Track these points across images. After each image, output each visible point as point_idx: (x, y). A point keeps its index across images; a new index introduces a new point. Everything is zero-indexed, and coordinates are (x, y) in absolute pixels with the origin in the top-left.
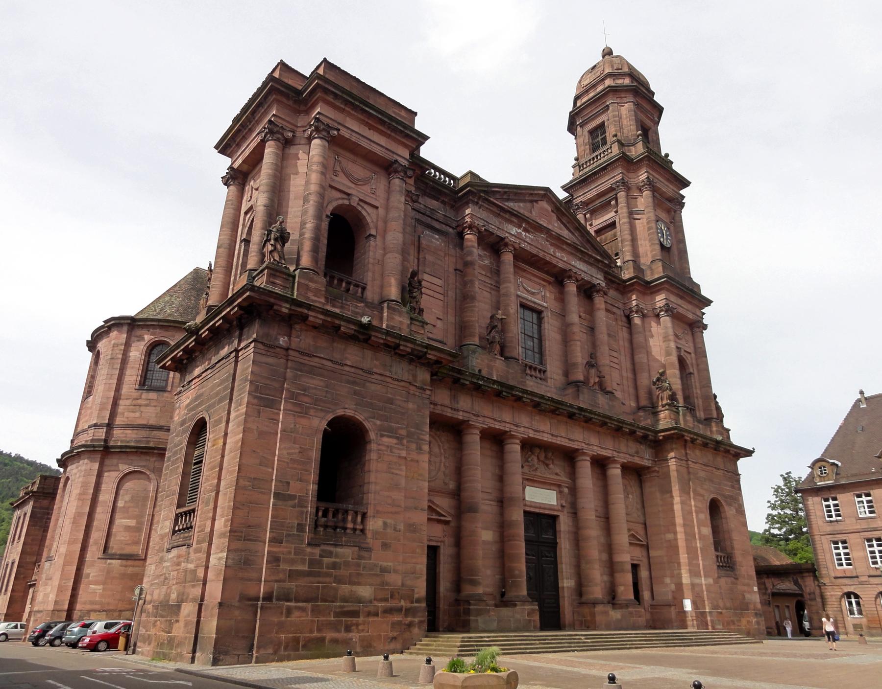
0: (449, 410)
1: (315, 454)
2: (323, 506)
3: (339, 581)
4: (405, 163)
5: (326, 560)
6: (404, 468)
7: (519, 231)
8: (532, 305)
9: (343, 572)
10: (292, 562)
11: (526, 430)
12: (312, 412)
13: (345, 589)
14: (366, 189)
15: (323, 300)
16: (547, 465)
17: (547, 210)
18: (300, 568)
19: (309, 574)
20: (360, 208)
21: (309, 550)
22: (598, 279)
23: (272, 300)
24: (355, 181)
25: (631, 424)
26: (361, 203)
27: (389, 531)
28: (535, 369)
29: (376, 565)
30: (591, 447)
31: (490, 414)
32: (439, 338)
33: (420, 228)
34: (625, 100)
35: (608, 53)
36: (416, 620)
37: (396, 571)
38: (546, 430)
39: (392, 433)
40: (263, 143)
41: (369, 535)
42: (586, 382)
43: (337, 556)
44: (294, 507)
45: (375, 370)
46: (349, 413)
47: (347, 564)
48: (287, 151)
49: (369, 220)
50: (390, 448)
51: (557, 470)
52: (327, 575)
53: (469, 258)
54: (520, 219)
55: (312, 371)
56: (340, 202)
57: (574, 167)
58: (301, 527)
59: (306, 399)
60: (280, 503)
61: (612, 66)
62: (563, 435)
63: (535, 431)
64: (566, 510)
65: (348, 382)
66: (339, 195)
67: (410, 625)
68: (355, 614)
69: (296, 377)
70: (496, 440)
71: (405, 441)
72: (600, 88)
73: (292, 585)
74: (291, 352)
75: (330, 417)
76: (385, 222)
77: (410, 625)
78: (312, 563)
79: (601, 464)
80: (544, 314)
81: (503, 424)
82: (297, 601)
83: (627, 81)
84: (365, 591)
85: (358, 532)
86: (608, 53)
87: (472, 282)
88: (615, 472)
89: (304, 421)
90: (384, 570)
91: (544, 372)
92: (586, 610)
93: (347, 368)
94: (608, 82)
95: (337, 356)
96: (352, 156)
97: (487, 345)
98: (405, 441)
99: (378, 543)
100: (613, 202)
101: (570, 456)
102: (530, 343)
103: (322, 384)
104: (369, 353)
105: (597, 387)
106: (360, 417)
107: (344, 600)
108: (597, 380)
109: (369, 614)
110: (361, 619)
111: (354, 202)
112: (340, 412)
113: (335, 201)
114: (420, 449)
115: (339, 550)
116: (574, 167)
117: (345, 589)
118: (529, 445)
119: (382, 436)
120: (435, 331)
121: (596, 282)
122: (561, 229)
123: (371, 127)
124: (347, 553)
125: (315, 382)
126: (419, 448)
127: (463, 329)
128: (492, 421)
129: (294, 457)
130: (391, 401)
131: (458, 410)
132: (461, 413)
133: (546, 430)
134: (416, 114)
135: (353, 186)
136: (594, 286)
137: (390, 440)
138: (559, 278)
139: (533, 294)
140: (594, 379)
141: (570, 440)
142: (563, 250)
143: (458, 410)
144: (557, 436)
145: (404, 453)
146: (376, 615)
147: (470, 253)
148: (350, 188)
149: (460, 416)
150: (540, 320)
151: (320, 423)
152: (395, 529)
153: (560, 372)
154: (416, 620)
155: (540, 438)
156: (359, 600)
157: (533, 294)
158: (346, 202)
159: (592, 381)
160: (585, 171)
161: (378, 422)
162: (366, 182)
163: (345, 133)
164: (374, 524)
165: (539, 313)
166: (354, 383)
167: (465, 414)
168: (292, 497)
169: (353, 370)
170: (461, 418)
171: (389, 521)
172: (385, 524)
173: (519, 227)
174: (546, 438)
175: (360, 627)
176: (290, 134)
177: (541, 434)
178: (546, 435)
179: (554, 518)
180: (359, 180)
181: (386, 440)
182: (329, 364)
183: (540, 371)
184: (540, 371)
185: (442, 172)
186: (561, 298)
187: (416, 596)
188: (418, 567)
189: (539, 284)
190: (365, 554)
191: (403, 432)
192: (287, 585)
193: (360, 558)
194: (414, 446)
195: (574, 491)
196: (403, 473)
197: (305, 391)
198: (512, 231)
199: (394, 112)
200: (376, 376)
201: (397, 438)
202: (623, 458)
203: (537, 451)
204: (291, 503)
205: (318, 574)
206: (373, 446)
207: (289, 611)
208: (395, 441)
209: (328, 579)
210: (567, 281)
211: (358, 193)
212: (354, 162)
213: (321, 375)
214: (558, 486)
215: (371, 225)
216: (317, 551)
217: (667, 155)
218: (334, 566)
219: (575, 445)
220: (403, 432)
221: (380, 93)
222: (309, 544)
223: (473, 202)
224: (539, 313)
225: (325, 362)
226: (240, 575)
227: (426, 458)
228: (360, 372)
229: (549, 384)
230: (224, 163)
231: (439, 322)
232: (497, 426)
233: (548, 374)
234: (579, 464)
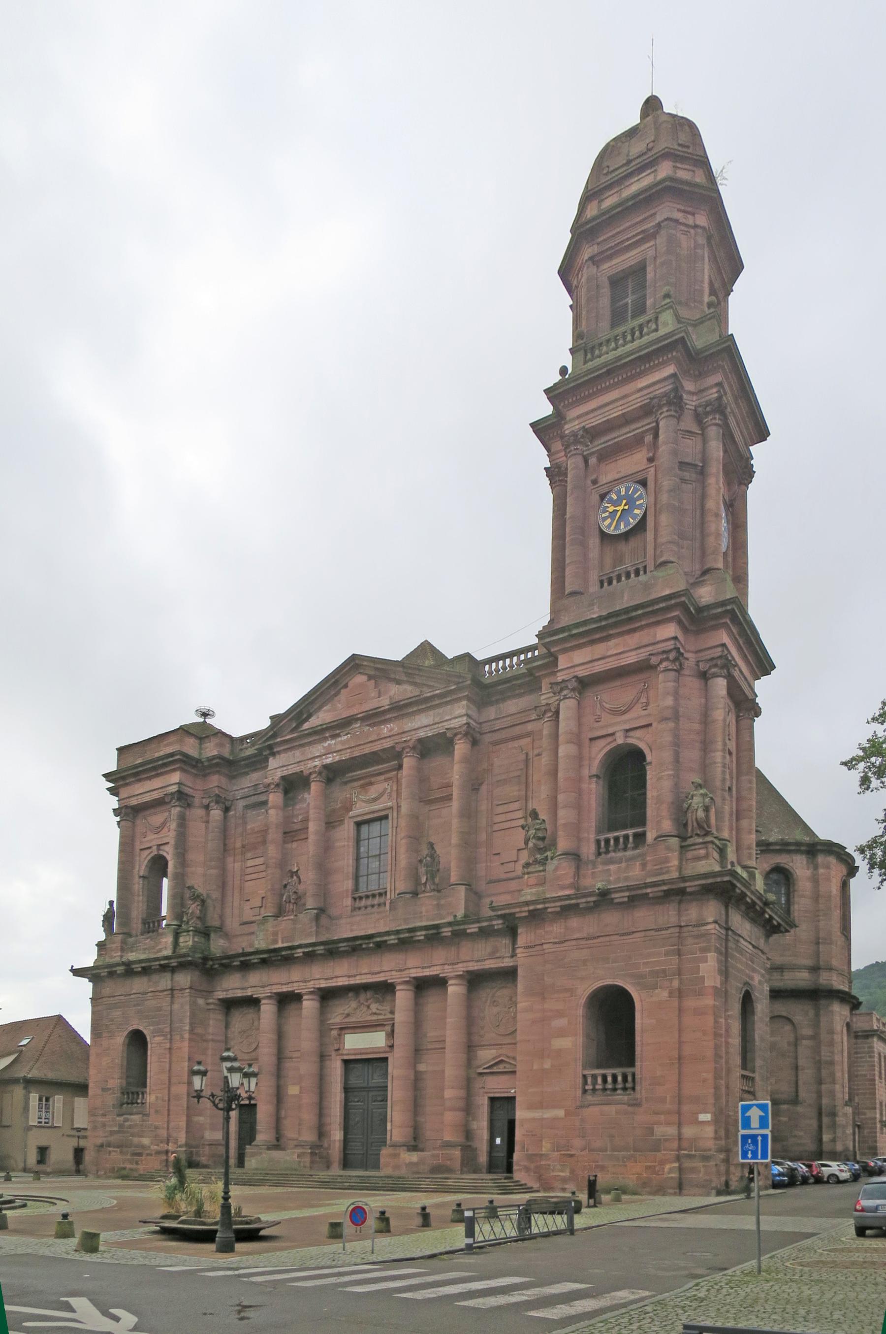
0: (239, 991)
3: (133, 1135)
5: (126, 1123)
6: (168, 1056)
7: (326, 744)
8: (371, 816)
11: (317, 982)
13: (136, 1140)
19: (118, 1132)
21: (118, 1118)
25: (450, 924)
30: (407, 972)
37: (163, 1128)
47: (136, 1125)
54: (320, 733)
59: (113, 1026)
63: (326, 979)
65: (134, 1006)
68: (140, 1154)
73: (111, 1139)
75: (126, 1033)
78: (121, 1126)
81: (291, 985)
82: (114, 1147)
84: (146, 1141)
90: (156, 1128)
93: (132, 996)
98: (169, 1036)
99: (152, 1111)
104: (145, 979)
106: (141, 1028)
107: (136, 1146)
109: (148, 1155)
110: (143, 1158)
112: (131, 1029)
115: (132, 1117)
117: (136, 1140)
124: (136, 1118)
126: (182, 1038)
128: (279, 986)
130: (159, 1009)
132: (249, 990)
141: (372, 974)
142: (388, 721)
144: (355, 976)
146: (151, 1155)
149: (249, 993)
152: (163, 1100)
155: (334, 984)
156: (143, 1147)
161: (152, 1028)
164: (150, 1098)
166: (138, 1005)
167: (253, 989)
168: (109, 1089)
170: (250, 994)
172: (157, 1097)
173: (326, 739)
177: (335, 980)
178: (341, 979)
181: (157, 1039)
182: (122, 997)
190: (145, 1118)
192: (109, 1139)
193: (143, 1121)
194: (178, 1037)
196: (167, 1060)
197: (112, 1021)
200: (149, 994)
201: (163, 1035)
202: (461, 969)
205: (124, 1132)
206: (149, 1046)
207: (110, 1152)
208: (162, 1038)
216: (121, 1118)
218: (130, 1127)
220: (168, 1030)
222: (119, 1115)
224: (386, 817)
227: (186, 1044)
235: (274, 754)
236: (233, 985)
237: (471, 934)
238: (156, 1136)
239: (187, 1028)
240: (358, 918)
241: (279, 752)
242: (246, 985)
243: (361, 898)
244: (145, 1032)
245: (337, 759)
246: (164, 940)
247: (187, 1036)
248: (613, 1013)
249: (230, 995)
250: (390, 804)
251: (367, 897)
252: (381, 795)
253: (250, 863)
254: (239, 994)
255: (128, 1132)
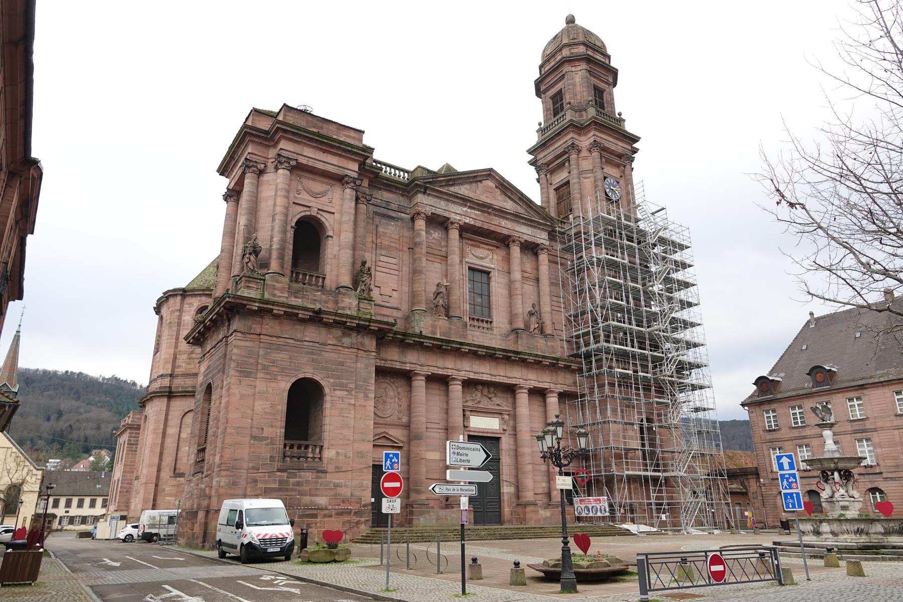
1: (283, 407)
2: (289, 442)
3: (302, 494)
4: (355, 175)
6: (353, 412)
7: (465, 209)
9: (305, 488)
10: (266, 482)
12: (279, 378)
13: (307, 499)
14: (325, 199)
15: (286, 295)
16: (490, 398)
17: (491, 188)
18: (273, 486)
20: (319, 216)
21: (278, 473)
22: (541, 237)
23: (245, 302)
24: (315, 195)
26: (320, 212)
27: (340, 457)
28: (482, 321)
29: (330, 482)
31: (434, 364)
32: (395, 306)
33: (377, 219)
34: (579, 68)
35: (571, 20)
36: (363, 519)
37: (346, 486)
38: (485, 371)
39: (343, 387)
40: (244, 173)
41: (325, 461)
42: (527, 327)
43: (300, 477)
44: (267, 445)
45: (329, 342)
46: (308, 376)
47: (307, 482)
48: (261, 178)
49: (327, 224)
50: (342, 398)
51: (500, 401)
52: (292, 490)
53: (417, 240)
54: (464, 201)
55: (279, 348)
56: (303, 214)
57: (538, 131)
58: (272, 458)
59: (274, 369)
60: (257, 443)
61: (569, 36)
62: (502, 374)
64: (507, 433)
65: (307, 353)
66: (303, 209)
67: (358, 523)
68: (314, 516)
69: (266, 354)
70: (441, 381)
71: (353, 393)
72: (559, 58)
74: (262, 337)
75: (294, 380)
76: (340, 224)
77: (358, 523)
78: (281, 482)
79: (539, 394)
80: (491, 275)
83: (581, 49)
84: (322, 501)
85: (317, 460)
86: (571, 20)
87: (420, 259)
88: (553, 400)
89: (273, 385)
90: (336, 486)
91: (491, 322)
92: (520, 510)
94: (566, 52)
95: (299, 336)
96: (311, 176)
97: (434, 309)
100: (567, 164)
101: (510, 390)
102: (479, 300)
103: (287, 356)
104: (324, 331)
105: (536, 331)
106: (317, 378)
108: (537, 326)
109: (325, 516)
110: (319, 519)
111: (314, 212)
112: (301, 376)
113: (297, 213)
114: (367, 397)
116: (538, 131)
117: (307, 499)
118: (469, 384)
119: (335, 390)
120: (391, 300)
121: (540, 241)
122: (505, 201)
123: (324, 151)
124: (308, 475)
125: (281, 356)
127: (413, 297)
129: (267, 410)
131: (405, 363)
133: (485, 371)
134: (363, 132)
135: (313, 199)
136: (538, 245)
137: (342, 392)
138: (504, 241)
139: (482, 258)
140: (533, 325)
143: (405, 363)
145: (352, 402)
146: (331, 516)
147: (419, 235)
148: (310, 201)
150: (489, 278)
151: (285, 385)
153: (506, 321)
154: (363, 519)
157: (482, 258)
158: (308, 213)
159: (532, 327)
160: (547, 135)
161: (332, 380)
162: (324, 194)
163: (302, 160)
164: (328, 454)
165: (488, 273)
166: (312, 353)
168: (266, 438)
169: (311, 344)
171: (340, 451)
172: (338, 453)
173: (465, 206)
174: (486, 377)
175: (318, 525)
176: (263, 166)
179: (498, 439)
180: (318, 194)
181: (338, 392)
182: (292, 341)
183: (487, 322)
184: (487, 322)
185: (396, 168)
186: (508, 259)
187: (363, 503)
188: (365, 482)
189: (488, 249)
191: (353, 386)
193: (318, 477)
194: (361, 395)
195: (514, 417)
196: (352, 416)
198: (458, 214)
199: (346, 136)
200: (329, 347)
201: (347, 391)
202: (560, 388)
203: (480, 387)
204: (265, 442)
205: (287, 490)
206: (328, 398)
208: (345, 393)
209: (293, 493)
210: (511, 245)
211: (315, 204)
212: (313, 180)
213: (286, 350)
214: (499, 413)
215: (329, 228)
216: (285, 474)
217: (620, 114)
218: (298, 484)
219: (513, 381)
220: (353, 386)
221: (332, 122)
222: (279, 470)
223: (421, 192)
224: (488, 273)
225: (288, 341)
226: (230, 492)
227: (372, 403)
228: (317, 345)
229: (495, 332)
230: (223, 184)
231: (394, 293)
232: (440, 372)
233: (494, 324)
234: (518, 396)
235: (424, 193)
236: (394, 358)
237: (497, 358)
238: (336, 495)
239: (373, 388)
240: (477, 333)
241: (429, 195)
242: (404, 360)
243: (473, 319)
244: (323, 383)
245: (472, 223)
246: (347, 300)
247: (372, 395)
248: (304, 401)
249: (388, 364)
250: (493, 266)
251: (478, 320)
252: (486, 258)
253: (382, 258)
254: (398, 366)
255: (296, 490)
